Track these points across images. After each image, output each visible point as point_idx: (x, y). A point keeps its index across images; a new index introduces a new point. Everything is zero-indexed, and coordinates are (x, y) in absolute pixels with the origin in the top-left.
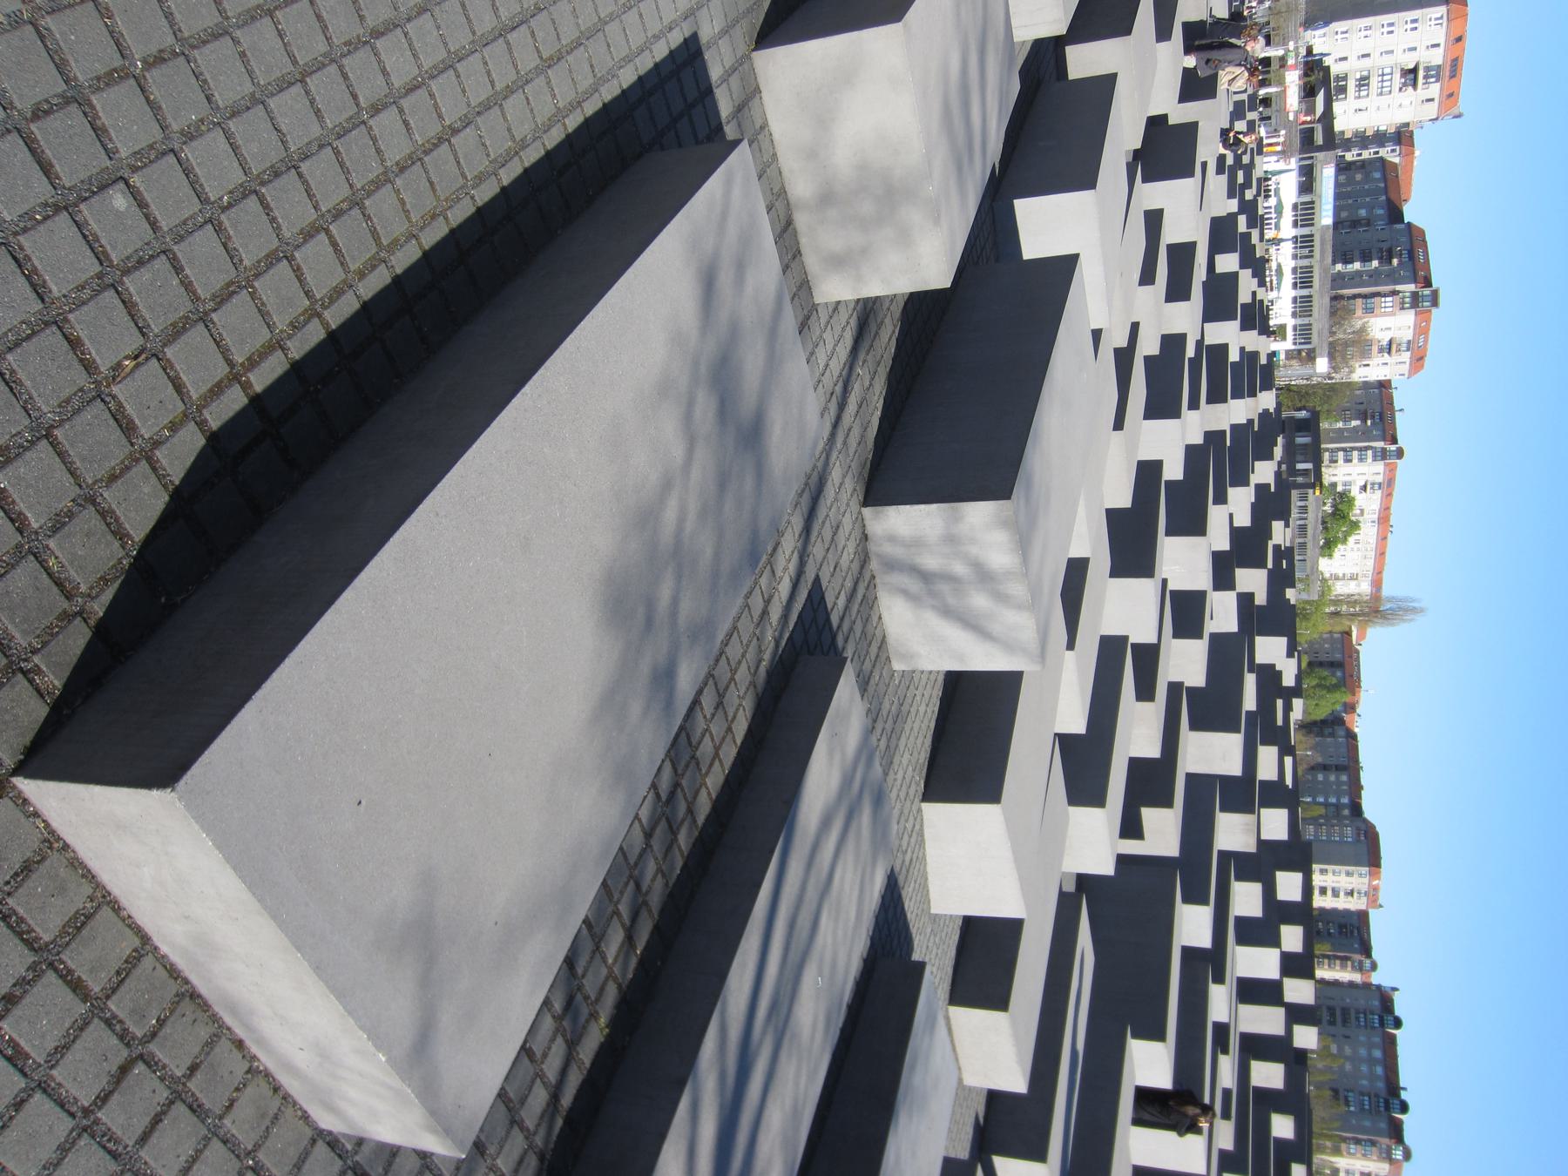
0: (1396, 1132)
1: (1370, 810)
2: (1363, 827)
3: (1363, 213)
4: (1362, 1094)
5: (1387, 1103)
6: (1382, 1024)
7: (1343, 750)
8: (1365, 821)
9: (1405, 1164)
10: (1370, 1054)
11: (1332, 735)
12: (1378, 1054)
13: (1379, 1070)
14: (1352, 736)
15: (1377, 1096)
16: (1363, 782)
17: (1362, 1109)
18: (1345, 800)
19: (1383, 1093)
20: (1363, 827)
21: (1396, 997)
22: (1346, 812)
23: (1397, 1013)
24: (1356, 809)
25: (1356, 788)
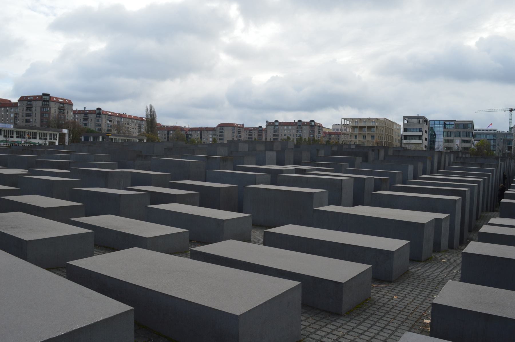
3: (12, 115)
5: (298, 126)
12: (285, 127)
13: (290, 127)
15: (297, 128)
18: (211, 132)
19: (296, 127)
21: (269, 121)
25: (207, 129)
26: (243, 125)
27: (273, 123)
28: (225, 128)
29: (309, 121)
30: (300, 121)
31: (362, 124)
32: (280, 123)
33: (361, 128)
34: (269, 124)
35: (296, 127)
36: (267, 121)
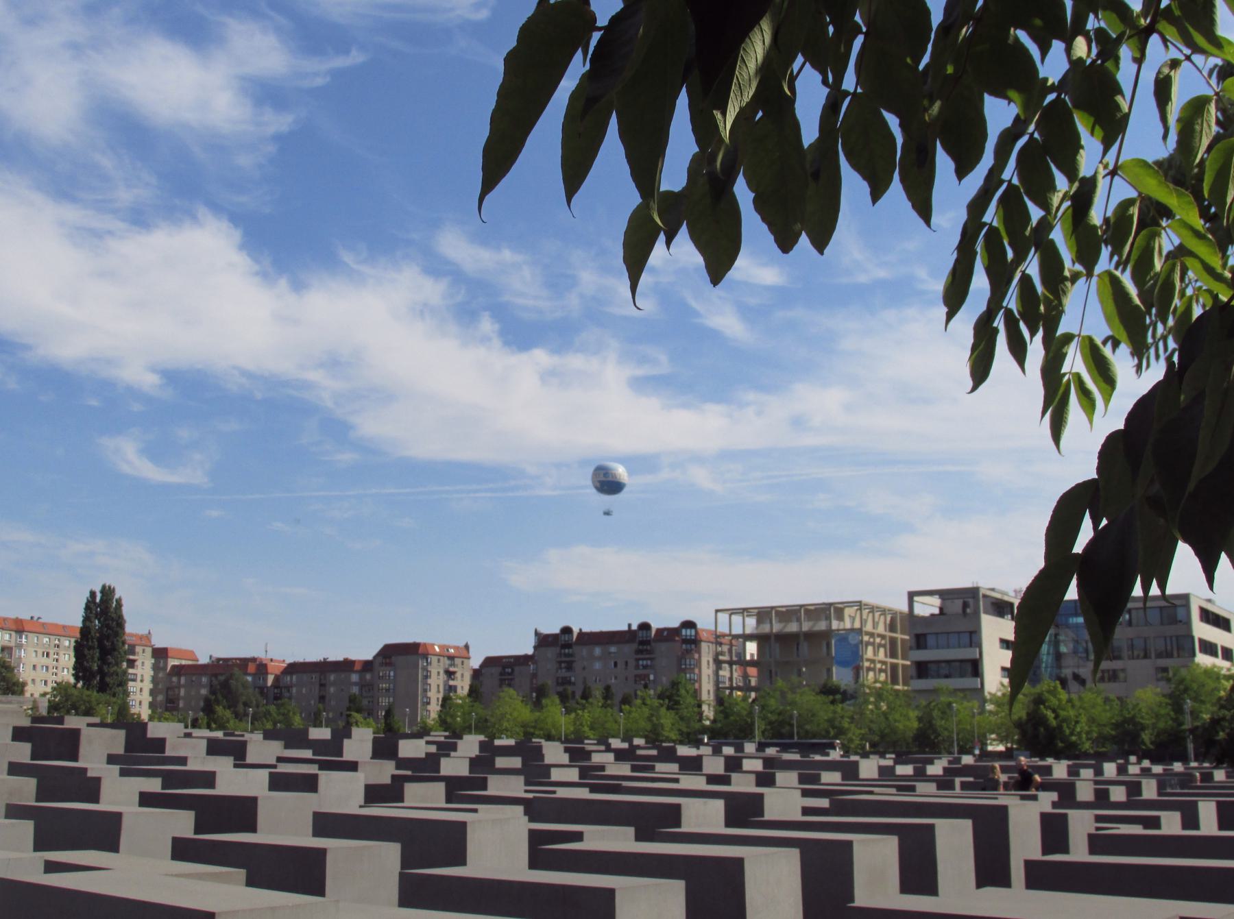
0: (668, 635)
1: (366, 652)
2: (380, 659)
4: (637, 667)
5: (642, 643)
6: (568, 645)
7: (305, 677)
8: (375, 657)
9: (699, 626)
10: (599, 659)
11: (289, 688)
12: (598, 651)
13: (613, 649)
14: (294, 668)
15: (638, 652)
16: (341, 659)
17: (651, 667)
19: (635, 646)
20: (380, 659)
22: (368, 676)
23: (557, 631)
24: (367, 665)
25: (346, 666)
26: (467, 647)
27: (555, 636)
28: (399, 660)
29: (675, 624)
30: (645, 627)
31: (793, 627)
32: (581, 634)
33: (783, 638)
34: (544, 641)
35: (635, 646)
36: (537, 633)
